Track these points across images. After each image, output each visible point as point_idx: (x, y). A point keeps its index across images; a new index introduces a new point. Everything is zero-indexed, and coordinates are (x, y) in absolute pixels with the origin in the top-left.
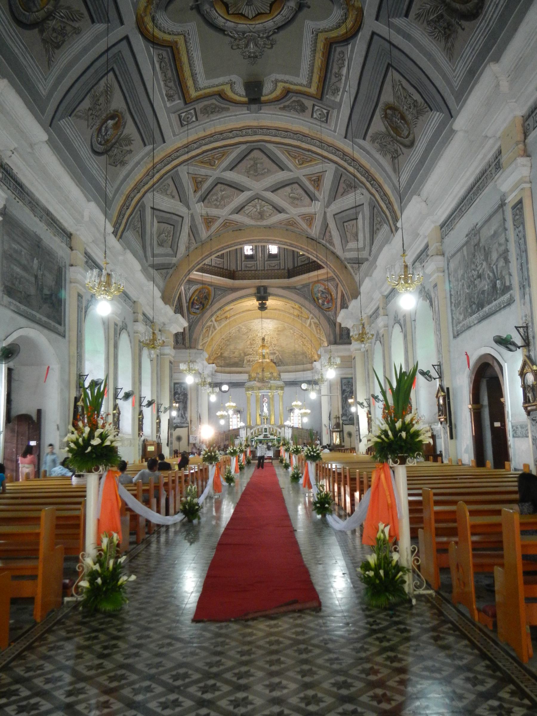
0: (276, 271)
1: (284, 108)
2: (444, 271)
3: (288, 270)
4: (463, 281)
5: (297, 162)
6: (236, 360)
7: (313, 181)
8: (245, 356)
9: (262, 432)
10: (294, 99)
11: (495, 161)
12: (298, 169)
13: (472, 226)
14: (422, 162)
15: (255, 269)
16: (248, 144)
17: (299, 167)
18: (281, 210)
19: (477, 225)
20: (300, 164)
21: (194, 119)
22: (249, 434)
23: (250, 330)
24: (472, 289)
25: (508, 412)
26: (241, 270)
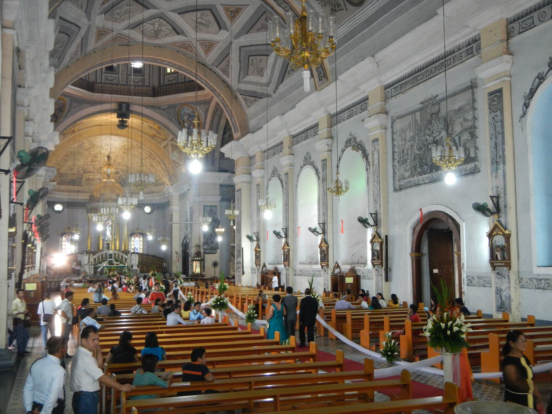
0: (140, 88)
2: (386, 129)
3: (154, 88)
4: (412, 142)
7: (230, 11)
8: (85, 173)
9: (106, 258)
11: (467, 46)
13: (430, 96)
14: (369, 22)
15: (117, 83)
19: (437, 96)
22: (92, 260)
23: (94, 146)
24: (424, 151)
25: (463, 264)
26: (101, 83)
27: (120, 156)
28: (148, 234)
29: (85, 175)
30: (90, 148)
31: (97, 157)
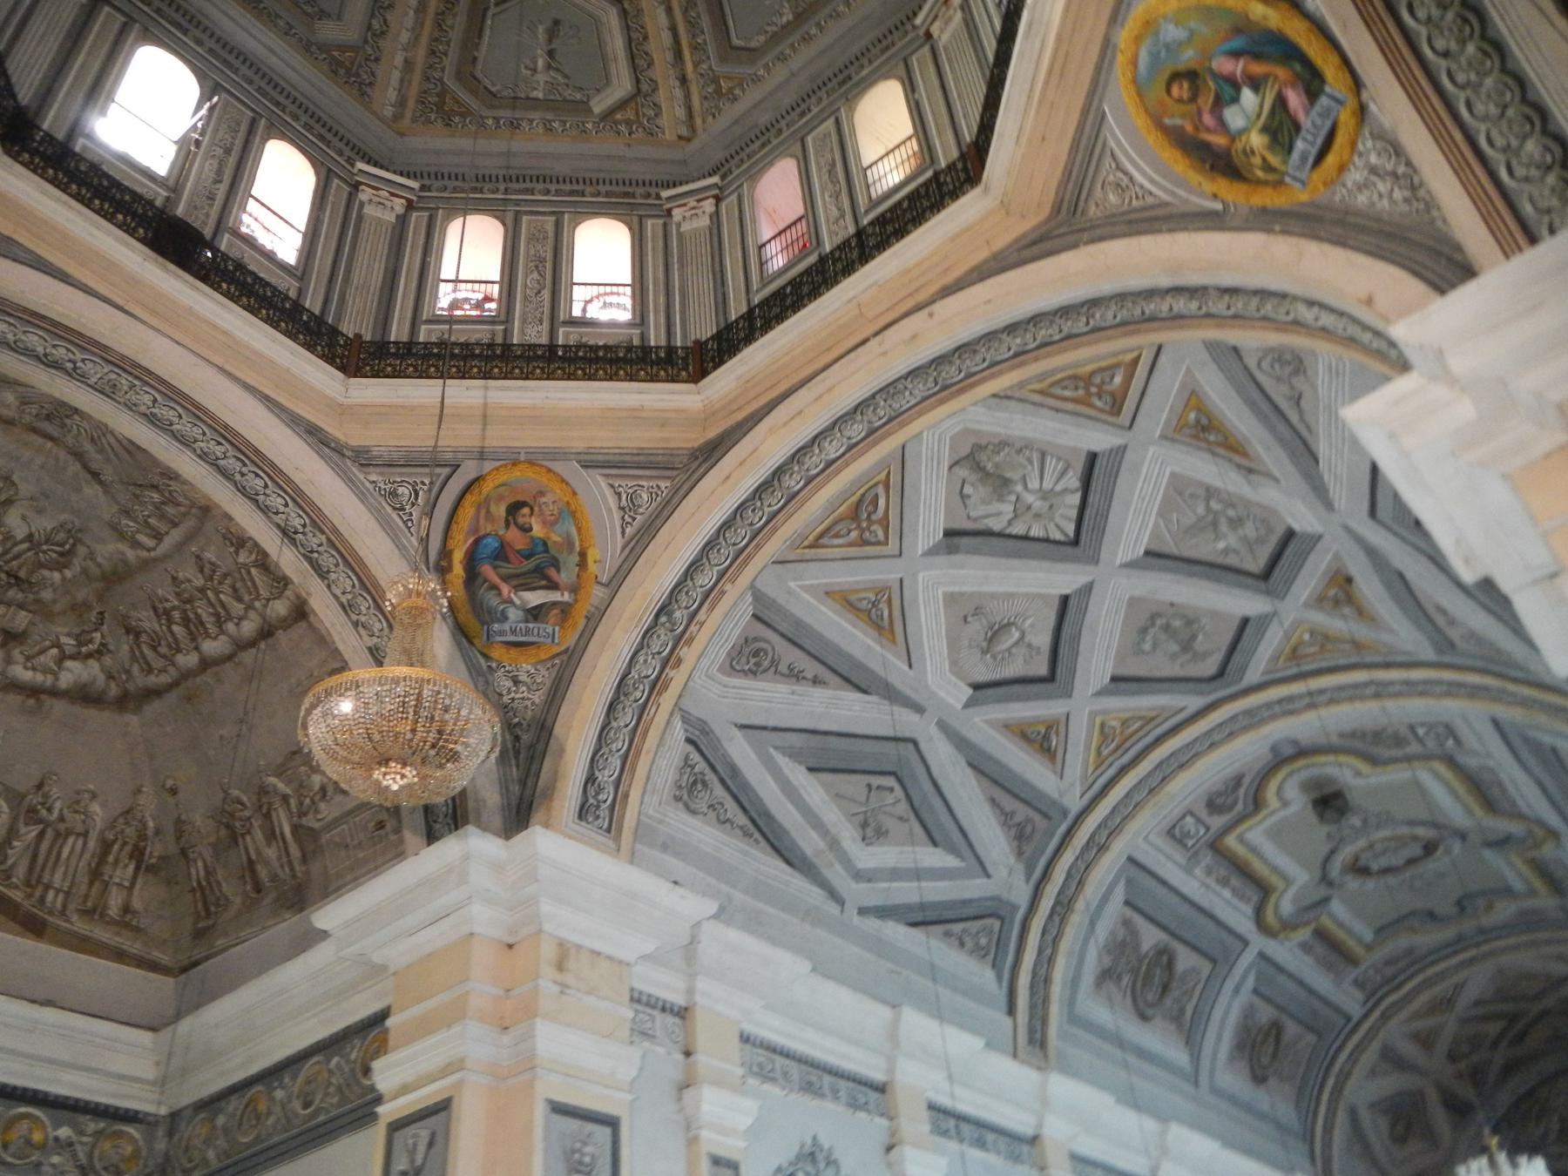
1: (1238, 780)
5: (1114, 723)
10: (1240, 806)
12: (1093, 715)
16: (1245, 683)
17: (1098, 721)
18: (956, 540)
20: (1103, 725)
21: (1421, 731)
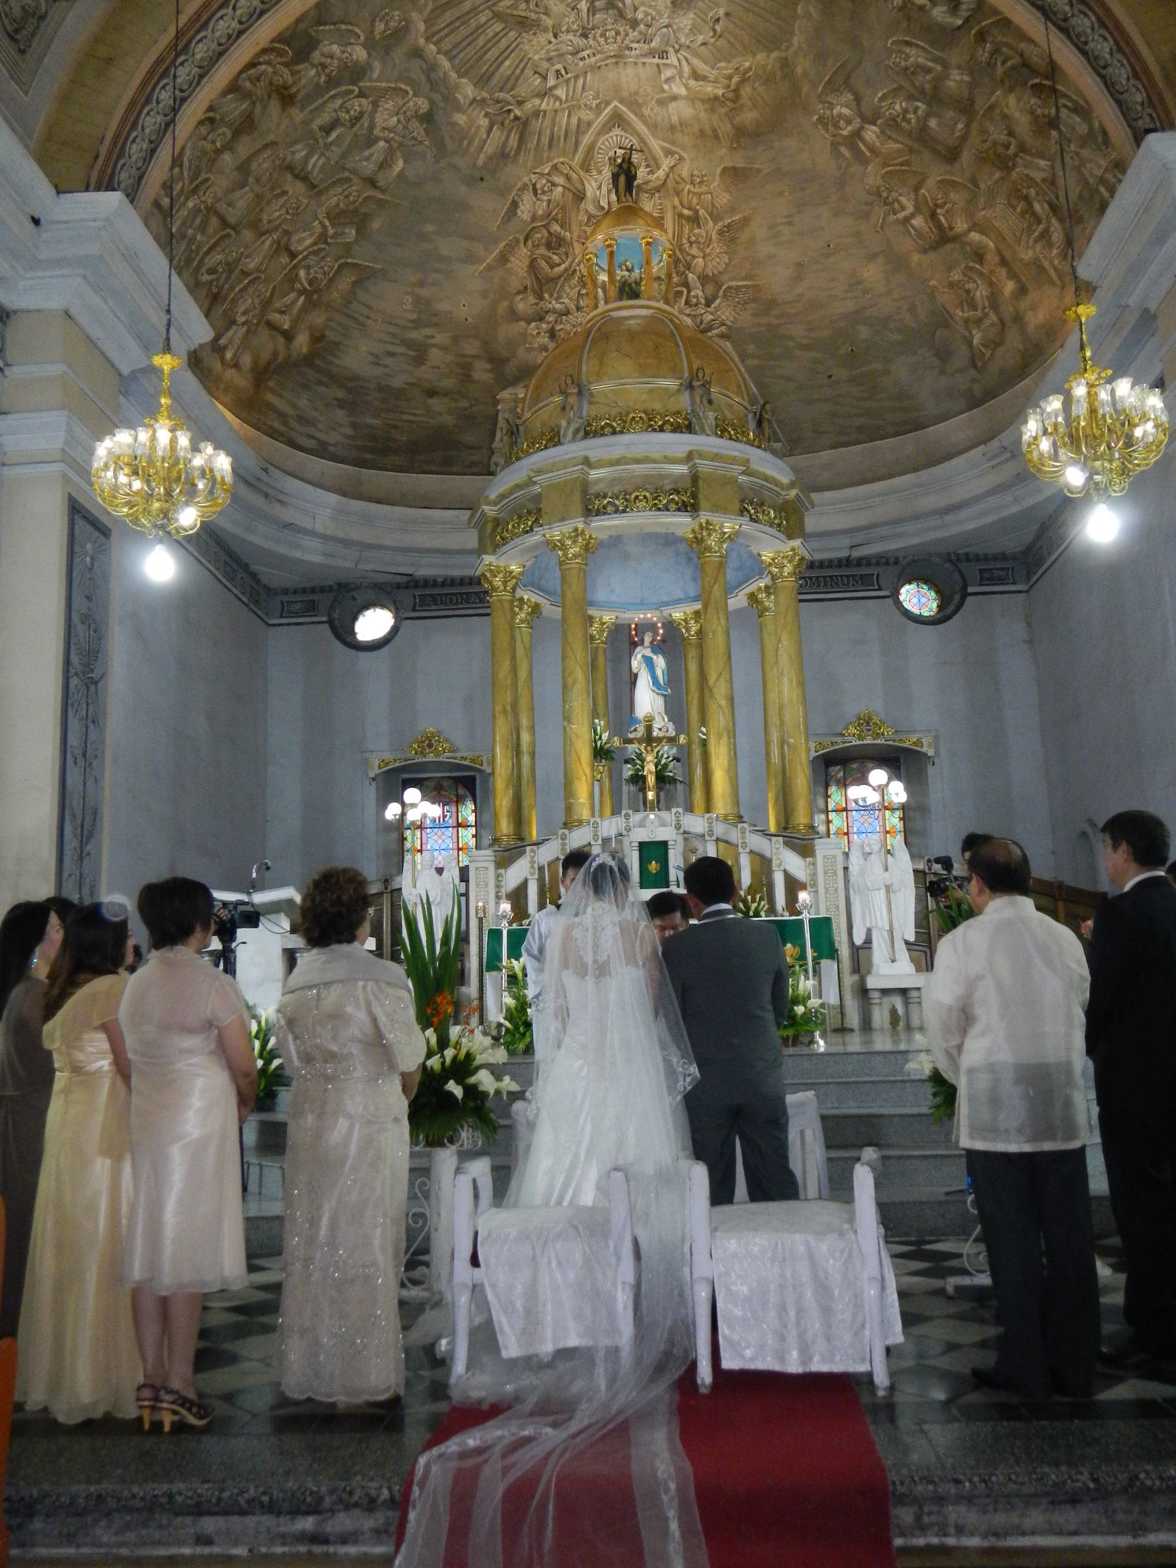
6: (441, 412)
8: (505, 382)
23: (523, 125)
27: (716, 218)
28: (1075, 477)
29: (505, 395)
30: (503, 156)
31: (561, 241)
